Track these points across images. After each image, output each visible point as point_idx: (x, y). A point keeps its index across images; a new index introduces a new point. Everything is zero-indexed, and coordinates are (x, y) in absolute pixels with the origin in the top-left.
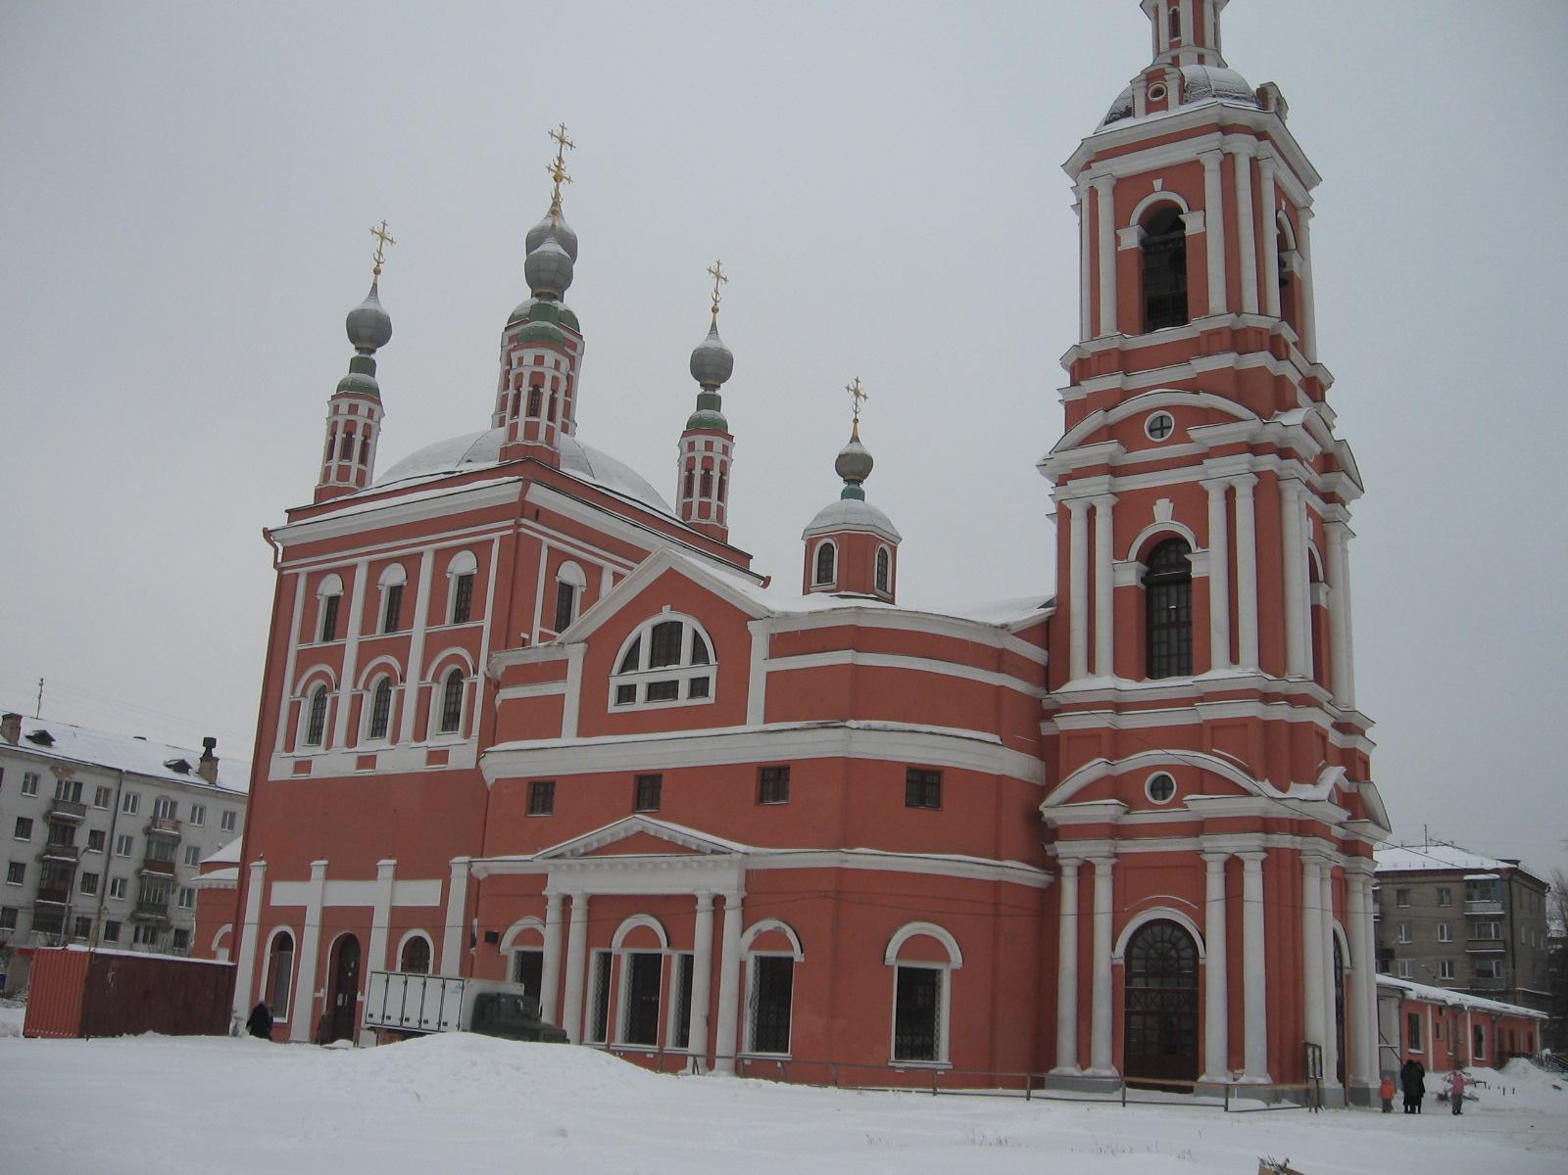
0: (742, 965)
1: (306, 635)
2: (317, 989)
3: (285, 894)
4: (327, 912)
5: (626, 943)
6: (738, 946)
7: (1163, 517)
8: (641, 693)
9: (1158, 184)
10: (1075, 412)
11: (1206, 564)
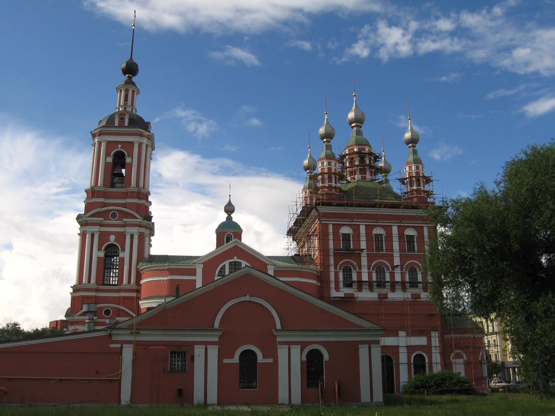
9: (120, 146)
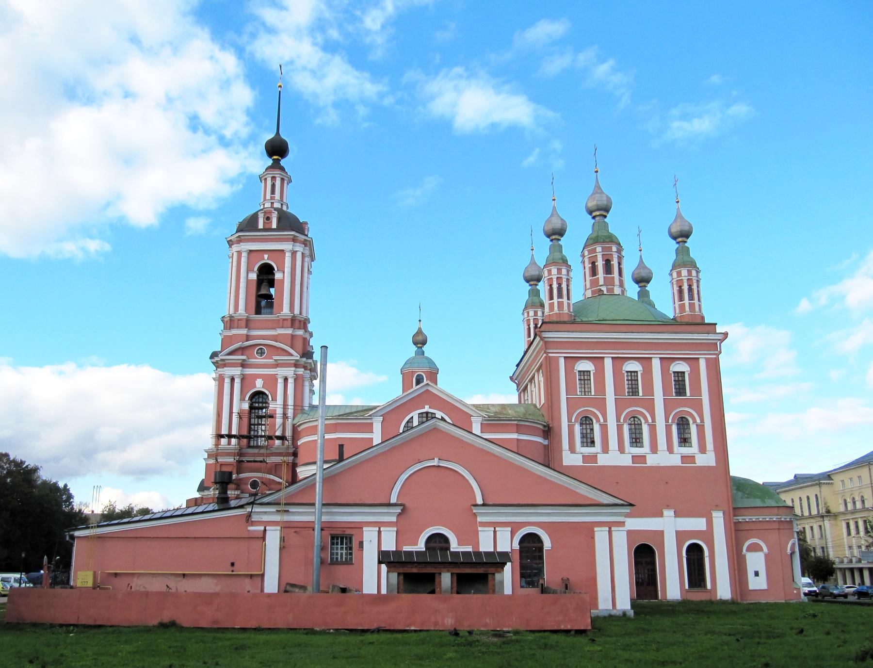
7: (259, 385)
9: (266, 256)
10: (226, 341)
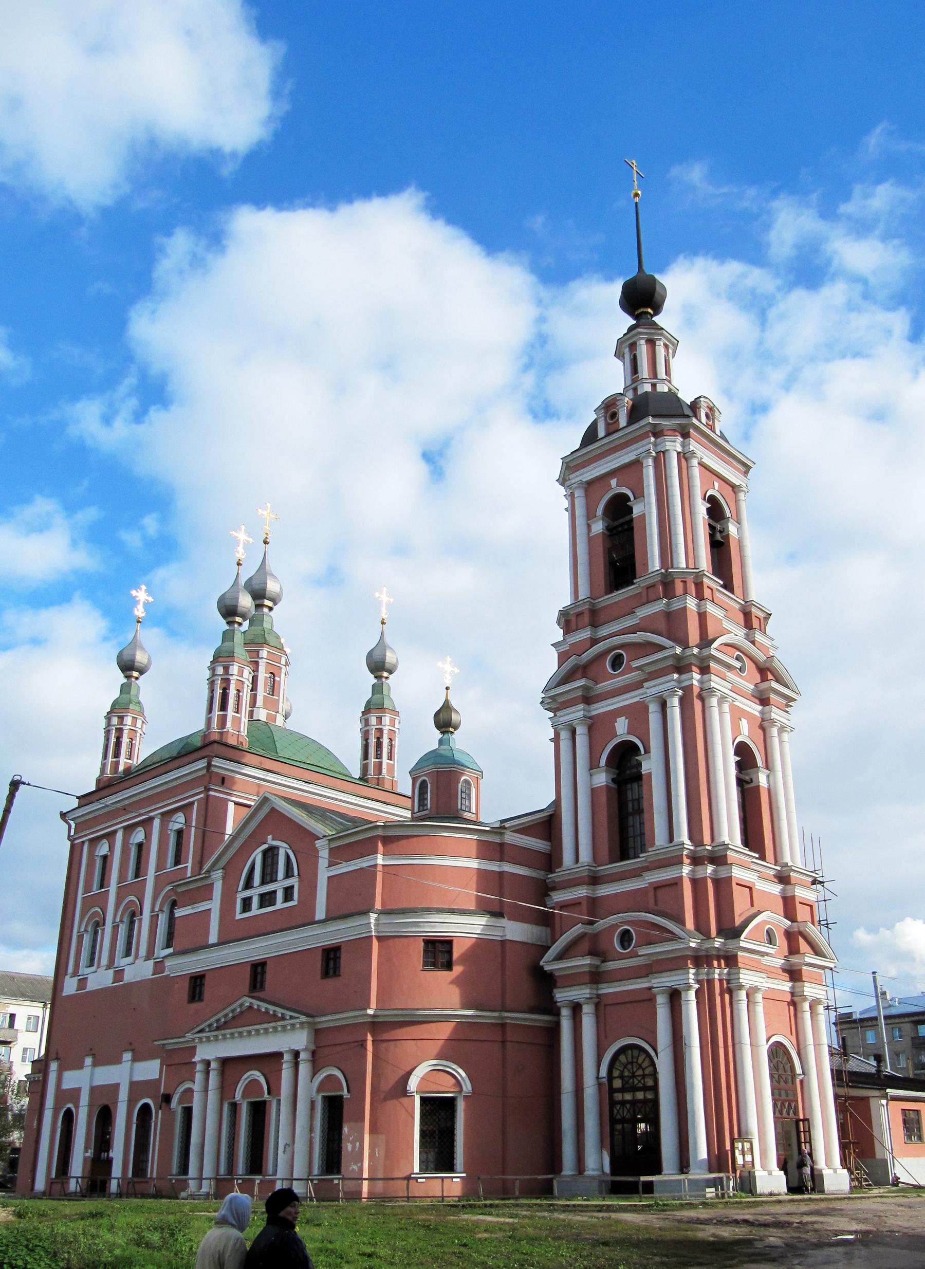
0: (313, 1103)
1: (87, 889)
2: (86, 1151)
3: (71, 1079)
4: (94, 1090)
5: (244, 1096)
6: (308, 1087)
8: (255, 902)
9: (614, 482)
11: (651, 765)
